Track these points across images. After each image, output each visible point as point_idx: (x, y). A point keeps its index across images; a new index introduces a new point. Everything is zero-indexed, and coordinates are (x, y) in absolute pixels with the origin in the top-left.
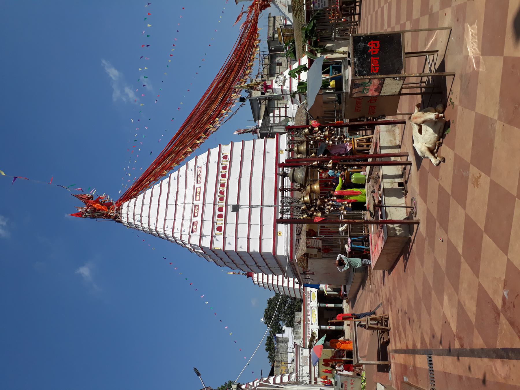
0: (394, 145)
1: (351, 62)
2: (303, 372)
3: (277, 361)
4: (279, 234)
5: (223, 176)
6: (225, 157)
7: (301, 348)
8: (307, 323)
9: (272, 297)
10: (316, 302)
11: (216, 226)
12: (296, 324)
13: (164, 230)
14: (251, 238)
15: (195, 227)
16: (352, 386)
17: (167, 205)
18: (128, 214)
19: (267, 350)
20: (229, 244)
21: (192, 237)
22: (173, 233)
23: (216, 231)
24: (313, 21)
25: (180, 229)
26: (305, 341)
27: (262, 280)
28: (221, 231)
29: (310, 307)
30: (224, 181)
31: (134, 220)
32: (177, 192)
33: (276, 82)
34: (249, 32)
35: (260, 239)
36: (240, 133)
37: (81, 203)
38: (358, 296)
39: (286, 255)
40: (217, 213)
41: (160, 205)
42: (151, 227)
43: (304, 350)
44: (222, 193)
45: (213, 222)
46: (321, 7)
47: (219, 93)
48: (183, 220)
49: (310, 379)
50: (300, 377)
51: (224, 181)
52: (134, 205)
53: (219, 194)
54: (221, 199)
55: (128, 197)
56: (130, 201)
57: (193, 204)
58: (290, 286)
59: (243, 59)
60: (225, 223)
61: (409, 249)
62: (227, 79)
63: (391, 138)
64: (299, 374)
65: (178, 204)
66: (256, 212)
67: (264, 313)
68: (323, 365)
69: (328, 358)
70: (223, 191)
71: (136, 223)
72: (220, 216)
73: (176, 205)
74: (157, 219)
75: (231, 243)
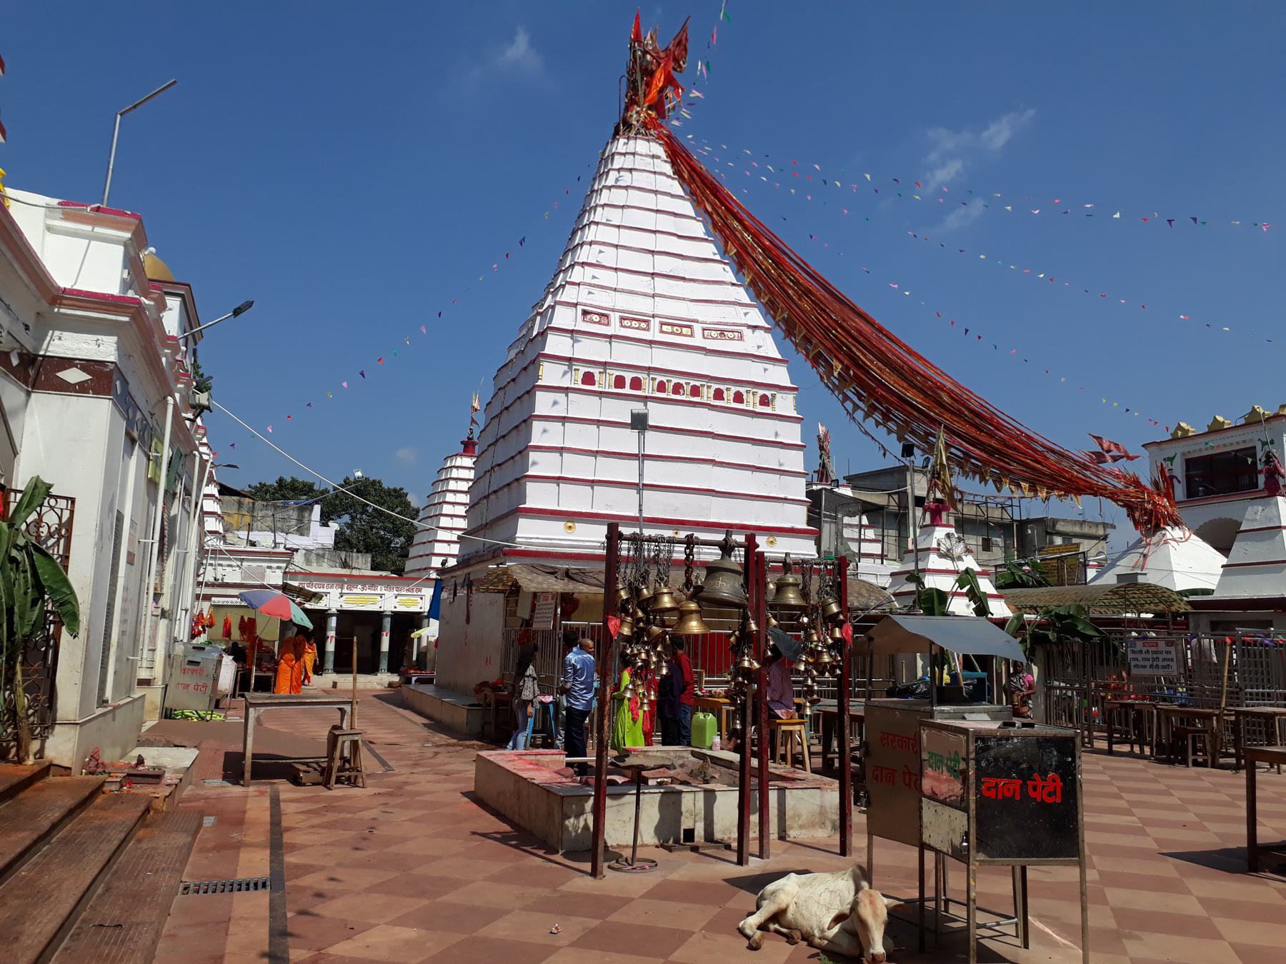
0: (787, 823)
1: (1011, 729)
2: (227, 568)
3: (254, 504)
4: (570, 524)
5: (719, 395)
7: (284, 565)
8: (346, 583)
9: (409, 498)
10: (395, 607)
11: (596, 371)
12: (343, 555)
13: (591, 243)
14: (561, 455)
15: (596, 318)
16: (191, 687)
17: (653, 252)
18: (634, 154)
19: (281, 481)
20: (555, 403)
21: (571, 311)
22: (583, 264)
23: (584, 369)
24: (1097, 634)
25: (594, 281)
26: (300, 576)
27: (456, 477)
28: (584, 382)
29: (383, 592)
30: (707, 395)
31: (619, 170)
32: (683, 279)
33: (948, 536)
34: (1073, 475)
35: (559, 478)
36: (820, 439)
37: (667, 41)
38: (407, 713)
39: (518, 540)
40: (628, 376)
41: (653, 235)
42: (599, 209)
43: (279, 573)
44: (677, 388)
45: (605, 365)
46: (1134, 656)
47: (924, 393)
48: (615, 290)
49: (207, 585)
50: (215, 559)
51: (707, 395)
52: (657, 170)
53: (675, 380)
54: (661, 387)
55: (677, 156)
56: (666, 161)
57: (653, 316)
58: (437, 545)
59: (1005, 455)
60: (601, 392)
61: (528, 848)
62: (959, 415)
63: (804, 817)
64: (220, 559)
65: (653, 278)
66: (627, 471)
67: (371, 479)
68: (242, 617)
69: (258, 632)
70: (681, 391)
71: (613, 175)
72: (620, 382)
73: (653, 274)
74: (619, 227)
75: (557, 406)
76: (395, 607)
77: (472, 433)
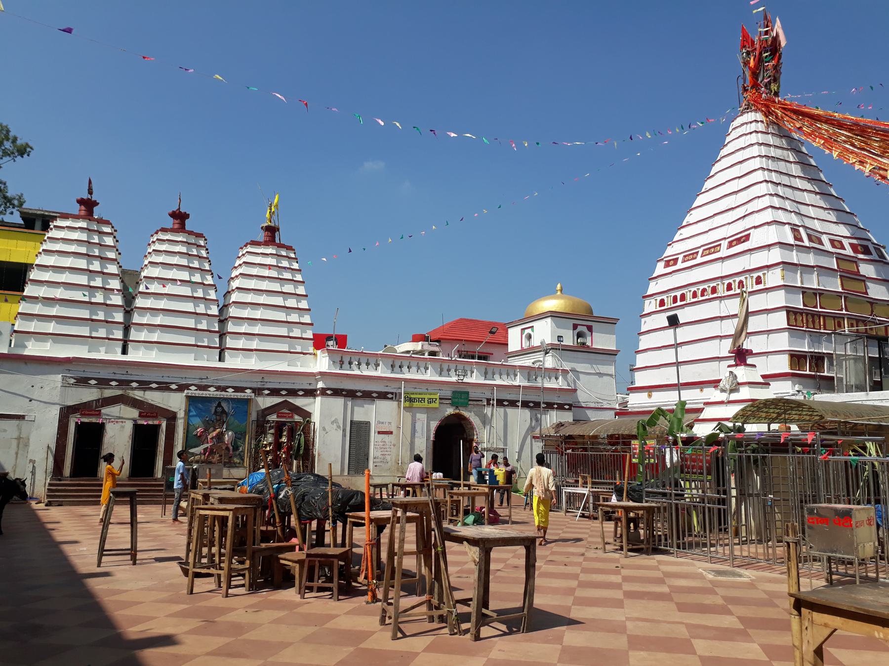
6: (759, 281)
28: (660, 306)
51: (722, 291)
53: (701, 287)
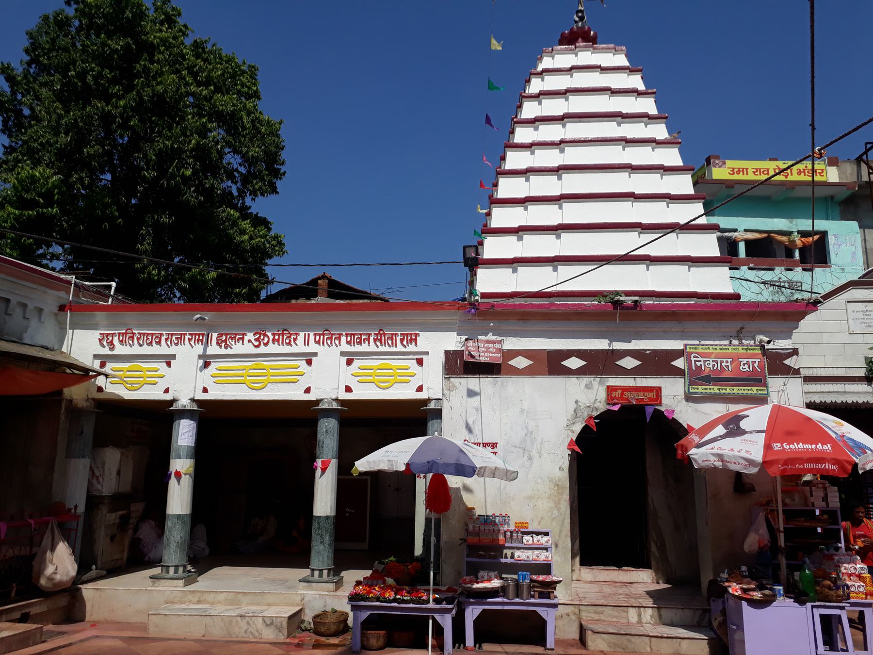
8: (212, 328)
10: (348, 389)
29: (313, 347)
76: (348, 389)
77: (581, 19)
